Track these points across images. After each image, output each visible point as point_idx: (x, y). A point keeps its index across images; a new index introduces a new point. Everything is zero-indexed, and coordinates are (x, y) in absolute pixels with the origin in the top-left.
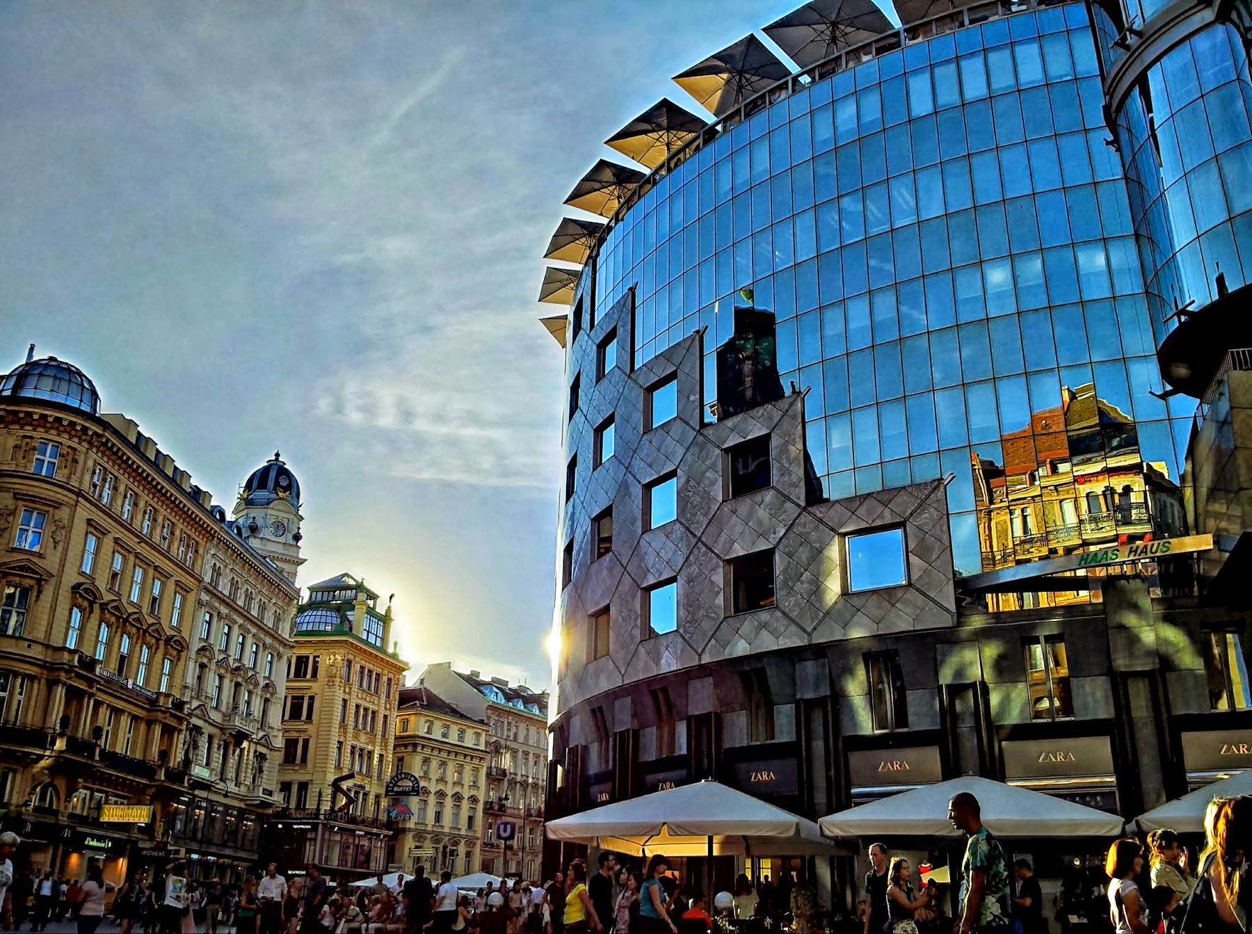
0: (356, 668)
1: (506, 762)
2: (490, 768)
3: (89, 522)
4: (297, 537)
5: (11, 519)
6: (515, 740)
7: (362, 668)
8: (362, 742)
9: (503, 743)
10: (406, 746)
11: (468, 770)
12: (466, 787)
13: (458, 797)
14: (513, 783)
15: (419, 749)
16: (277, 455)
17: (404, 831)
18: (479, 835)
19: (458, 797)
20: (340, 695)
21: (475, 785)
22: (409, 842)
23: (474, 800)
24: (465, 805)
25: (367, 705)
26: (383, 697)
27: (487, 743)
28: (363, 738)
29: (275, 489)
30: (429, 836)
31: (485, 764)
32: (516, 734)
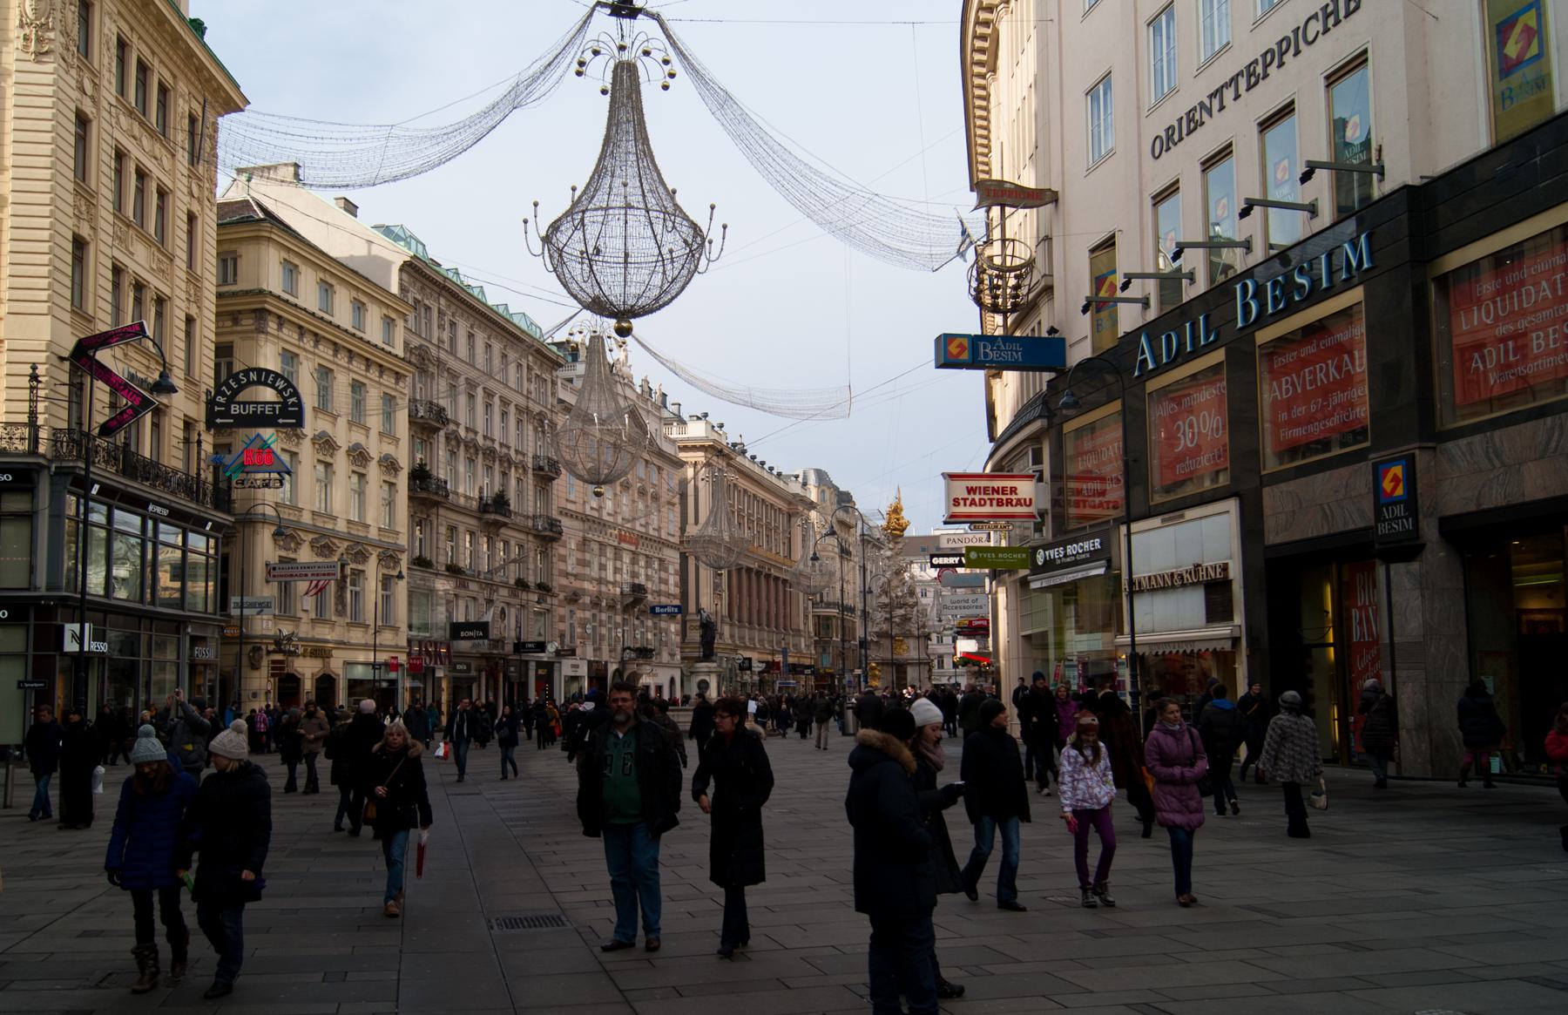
1: (440, 392)
2: (413, 401)
6: (452, 351)
7: (122, 45)
8: (140, 260)
9: (433, 351)
10: (235, 317)
11: (373, 397)
12: (374, 434)
13: (359, 455)
14: (453, 438)
15: (272, 326)
17: (249, 521)
18: (403, 541)
19: (359, 455)
21: (388, 434)
22: (266, 548)
23: (390, 465)
24: (374, 472)
25: (150, 164)
26: (183, 157)
27: (406, 344)
28: (140, 250)
30: (309, 537)
32: (453, 340)
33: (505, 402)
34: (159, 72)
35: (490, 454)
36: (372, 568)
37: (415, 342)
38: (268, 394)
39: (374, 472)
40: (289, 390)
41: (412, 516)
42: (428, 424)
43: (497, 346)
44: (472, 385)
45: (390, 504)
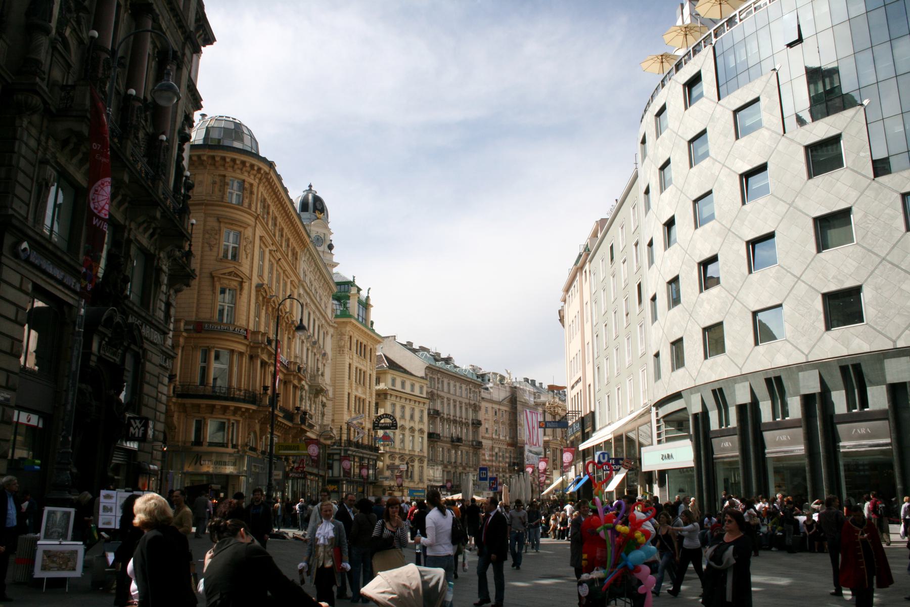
0: (354, 341)
2: (429, 409)
3: (261, 238)
4: (331, 247)
5: (217, 237)
6: (443, 391)
8: (360, 393)
9: (435, 391)
13: (412, 430)
15: (389, 397)
16: (310, 186)
18: (426, 455)
20: (347, 361)
24: (416, 434)
27: (427, 393)
29: (314, 212)
31: (426, 407)
33: (461, 403)
34: (365, 342)
35: (455, 421)
36: (416, 464)
37: (430, 390)
38: (388, 421)
39: (416, 434)
40: (394, 419)
41: (429, 446)
42: (434, 415)
43: (458, 384)
44: (449, 399)
45: (422, 443)
